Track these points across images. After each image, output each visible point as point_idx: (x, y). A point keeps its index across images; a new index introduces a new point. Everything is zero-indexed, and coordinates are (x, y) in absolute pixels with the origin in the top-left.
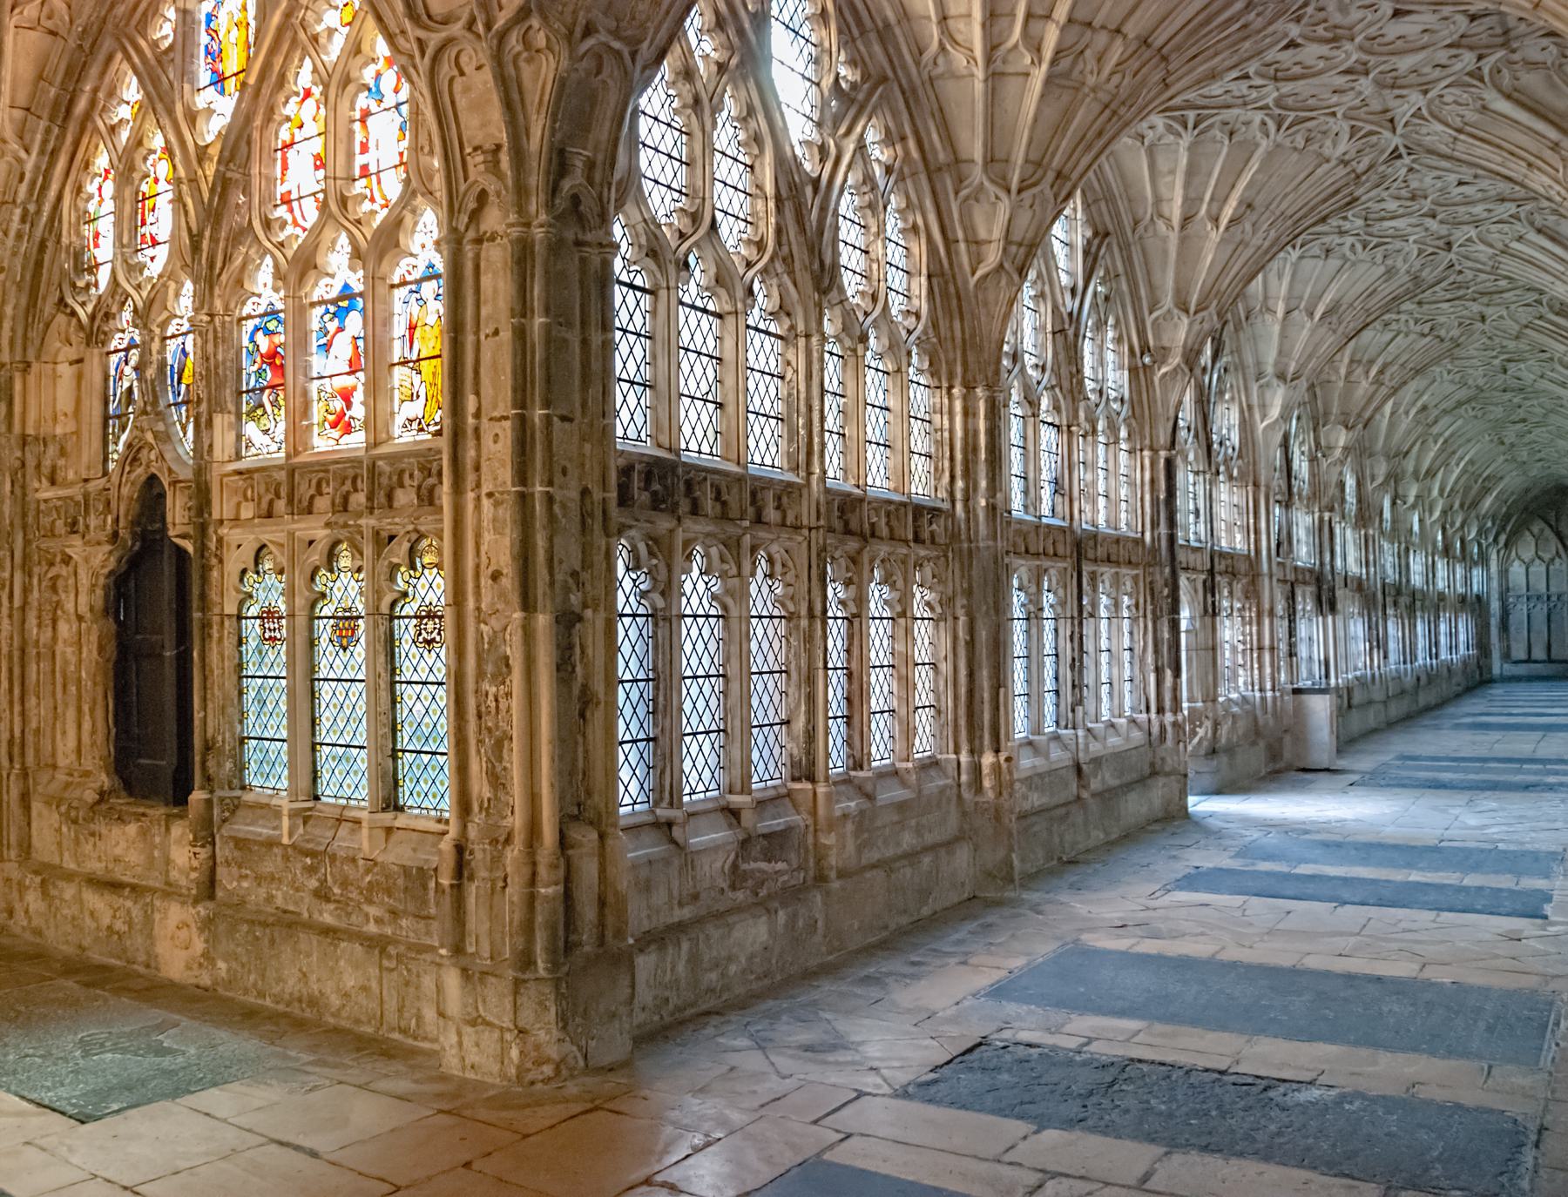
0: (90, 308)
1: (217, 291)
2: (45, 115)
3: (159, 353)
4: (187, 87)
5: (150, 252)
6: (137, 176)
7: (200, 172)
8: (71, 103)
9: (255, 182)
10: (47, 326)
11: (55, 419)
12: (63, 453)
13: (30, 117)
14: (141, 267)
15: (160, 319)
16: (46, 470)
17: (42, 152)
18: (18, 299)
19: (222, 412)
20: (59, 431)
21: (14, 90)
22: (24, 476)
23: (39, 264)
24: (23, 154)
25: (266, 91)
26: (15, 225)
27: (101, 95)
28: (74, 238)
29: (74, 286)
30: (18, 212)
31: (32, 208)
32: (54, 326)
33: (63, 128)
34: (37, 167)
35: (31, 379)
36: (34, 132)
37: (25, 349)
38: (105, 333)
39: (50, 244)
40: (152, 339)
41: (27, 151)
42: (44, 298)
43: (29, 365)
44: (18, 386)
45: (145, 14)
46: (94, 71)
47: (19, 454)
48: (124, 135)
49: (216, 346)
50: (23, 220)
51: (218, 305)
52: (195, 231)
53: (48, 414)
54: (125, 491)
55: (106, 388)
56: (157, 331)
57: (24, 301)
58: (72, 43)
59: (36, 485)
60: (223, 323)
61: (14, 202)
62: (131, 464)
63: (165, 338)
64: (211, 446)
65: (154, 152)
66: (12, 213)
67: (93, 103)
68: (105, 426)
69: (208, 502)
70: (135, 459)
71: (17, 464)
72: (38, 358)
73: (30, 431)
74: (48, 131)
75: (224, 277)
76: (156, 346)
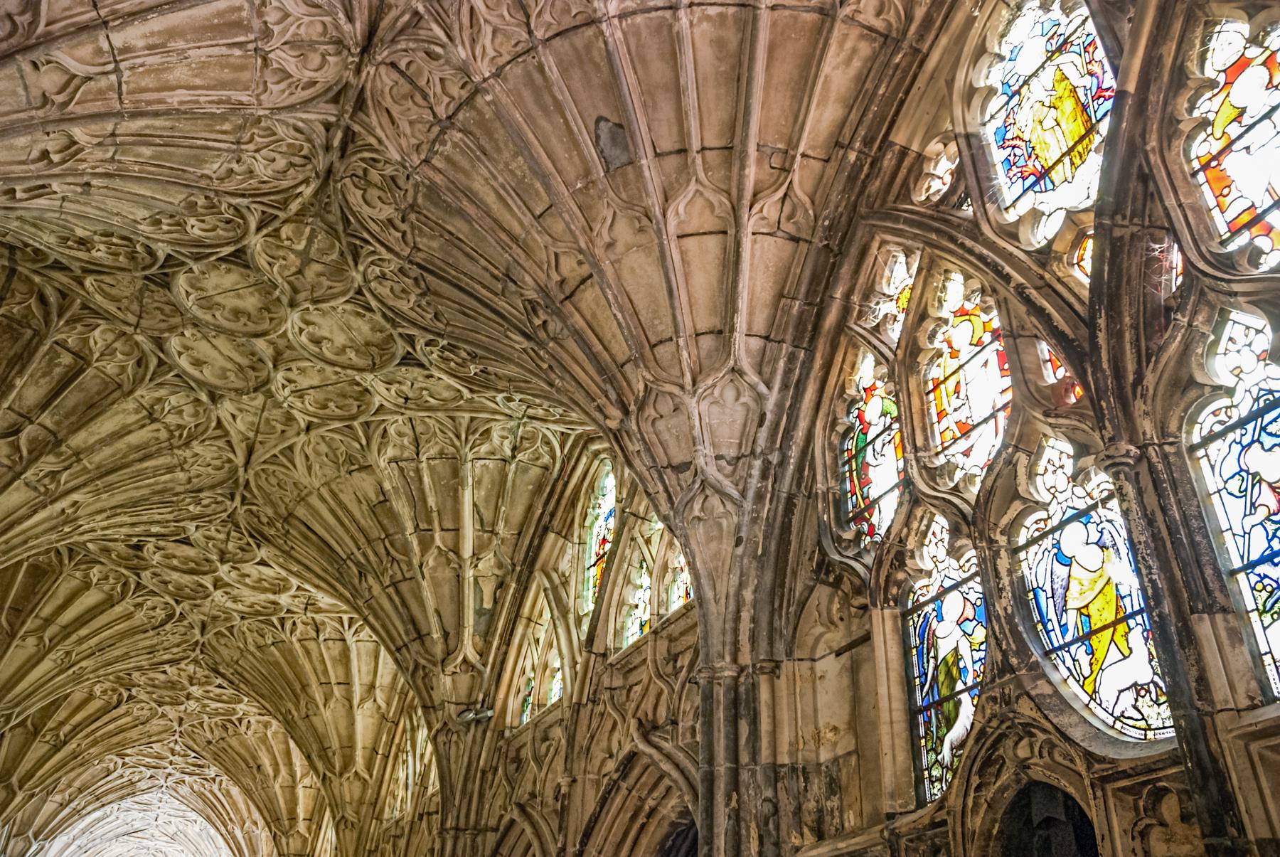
0: (869, 559)
1: (1139, 407)
2: (789, 338)
3: (1010, 572)
4: (991, 208)
5: (963, 445)
6: (923, 359)
7: (1047, 276)
8: (820, 316)
9: (1177, 215)
10: (803, 604)
11: (818, 738)
12: (834, 787)
13: (769, 345)
14: (950, 469)
15: (1005, 521)
16: (809, 819)
17: (785, 386)
18: (760, 577)
19: (1210, 609)
20: (825, 755)
21: (751, 314)
22: (777, 827)
23: (786, 529)
24: (762, 388)
25: (1155, 97)
26: (754, 482)
27: (855, 298)
28: (832, 483)
29: (839, 540)
30: (758, 463)
31: (775, 458)
32: (812, 602)
33: (811, 352)
34: (779, 406)
35: (782, 683)
36: (776, 360)
37: (771, 643)
38: (899, 584)
39: (799, 502)
40: (996, 554)
41: (768, 385)
42: (794, 573)
43: (778, 665)
44: (764, 694)
45: (905, 183)
46: (846, 271)
47: (769, 793)
48: (894, 333)
49: (1160, 493)
50: (764, 476)
51: (1147, 427)
52: (1087, 319)
53: (808, 731)
54: (976, 822)
55: (907, 665)
56: (1003, 540)
57: (768, 577)
58: (818, 242)
59: (796, 841)
60: (1165, 457)
61: (753, 452)
62: (981, 773)
63: (1015, 551)
64: (1202, 680)
65: (946, 322)
66: (750, 467)
67: (846, 311)
68: (912, 725)
69: (1227, 801)
70: (987, 762)
71: (768, 808)
72: (789, 654)
73: (784, 759)
74: (791, 358)
75: (1150, 379)
76: (1003, 563)
